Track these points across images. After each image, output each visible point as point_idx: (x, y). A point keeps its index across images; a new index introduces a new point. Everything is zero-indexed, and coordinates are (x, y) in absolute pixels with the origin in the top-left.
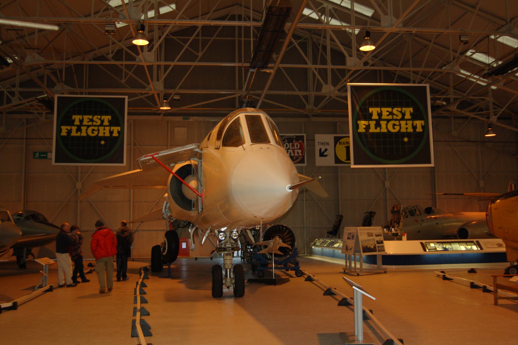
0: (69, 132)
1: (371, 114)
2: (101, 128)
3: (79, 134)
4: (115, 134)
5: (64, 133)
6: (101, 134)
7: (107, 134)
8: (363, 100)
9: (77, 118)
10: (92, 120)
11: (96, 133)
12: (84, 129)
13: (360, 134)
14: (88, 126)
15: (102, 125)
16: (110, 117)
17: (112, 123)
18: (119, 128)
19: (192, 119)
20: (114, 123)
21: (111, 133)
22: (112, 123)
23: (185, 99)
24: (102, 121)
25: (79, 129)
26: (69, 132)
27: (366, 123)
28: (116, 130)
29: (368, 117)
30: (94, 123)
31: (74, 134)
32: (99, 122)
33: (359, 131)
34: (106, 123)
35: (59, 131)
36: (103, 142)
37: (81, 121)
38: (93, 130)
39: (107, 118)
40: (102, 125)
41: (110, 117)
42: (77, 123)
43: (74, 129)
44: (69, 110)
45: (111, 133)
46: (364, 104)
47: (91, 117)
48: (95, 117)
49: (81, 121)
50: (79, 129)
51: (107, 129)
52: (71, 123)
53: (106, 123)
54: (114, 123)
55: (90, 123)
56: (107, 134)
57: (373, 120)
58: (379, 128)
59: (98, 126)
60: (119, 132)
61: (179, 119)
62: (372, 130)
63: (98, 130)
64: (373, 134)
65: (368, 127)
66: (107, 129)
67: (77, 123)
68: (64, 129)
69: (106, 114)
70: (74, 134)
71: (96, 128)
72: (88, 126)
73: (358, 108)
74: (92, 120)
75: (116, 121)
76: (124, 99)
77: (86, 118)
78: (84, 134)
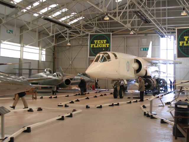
0: (93, 46)
1: (185, 39)
2: (103, 44)
3: (96, 47)
4: (108, 46)
5: (92, 47)
6: (103, 47)
7: (105, 46)
8: (181, 34)
9: (96, 41)
10: (100, 42)
11: (101, 46)
12: (98, 45)
13: (180, 46)
14: (99, 44)
15: (103, 43)
16: (106, 41)
17: (107, 43)
18: (109, 44)
19: (148, 35)
20: (107, 42)
21: (106, 46)
22: (107, 43)
23: (141, 29)
24: (104, 42)
25: (96, 45)
26: (93, 46)
27: (183, 42)
28: (108, 45)
29: (184, 40)
30: (101, 43)
31: (95, 47)
32: (102, 42)
33: (180, 45)
34: (105, 43)
35: (90, 46)
36: (104, 49)
37: (97, 42)
38: (101, 45)
39: (105, 41)
40: (103, 43)
41: (106, 41)
42: (96, 43)
43: (95, 45)
44: (94, 38)
45: (106, 46)
46: (182, 35)
47: (100, 41)
48: (101, 41)
49: (97, 42)
50: (96, 45)
51: (105, 44)
52: (94, 43)
53: (105, 43)
54: (107, 42)
55: (100, 43)
56: (105, 46)
57: (185, 41)
58: (187, 44)
59: (102, 44)
60: (109, 46)
61: (143, 35)
62: (185, 45)
63: (102, 45)
64: (185, 46)
65: (183, 44)
66: (105, 44)
67: (96, 43)
68: (92, 45)
69: (105, 39)
70: (95, 47)
71: (102, 44)
72: (99, 44)
73: (180, 36)
74: (100, 42)
75: (108, 42)
76: (110, 34)
77: (98, 41)
78: (98, 47)
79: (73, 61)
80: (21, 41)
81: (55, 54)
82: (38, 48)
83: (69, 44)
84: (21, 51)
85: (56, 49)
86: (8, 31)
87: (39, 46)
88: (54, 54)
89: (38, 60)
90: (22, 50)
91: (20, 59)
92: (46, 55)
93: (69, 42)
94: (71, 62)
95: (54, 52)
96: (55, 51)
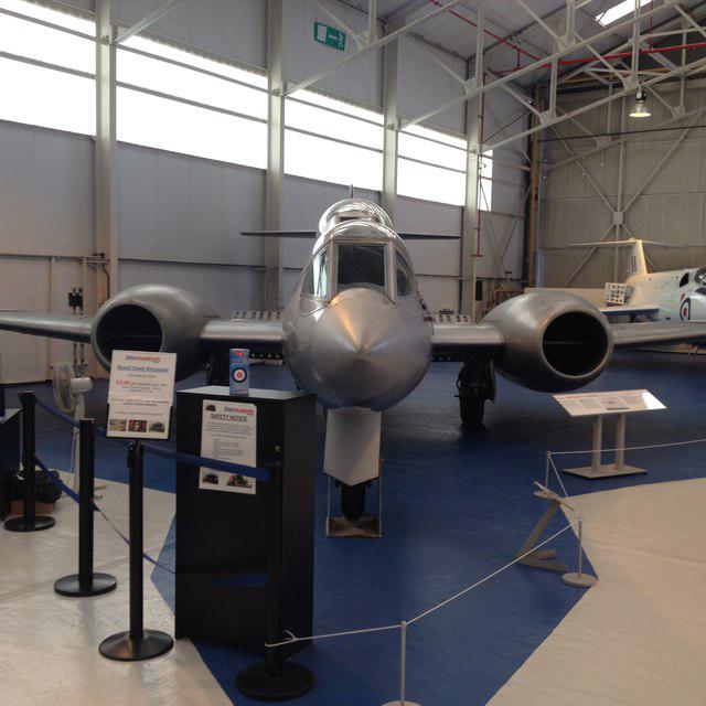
79: (629, 209)
80: (382, 92)
81: (533, 178)
82: (463, 143)
83: (640, 113)
84: (384, 152)
85: (538, 151)
86: (322, 32)
87: (465, 133)
88: (527, 177)
89: (462, 203)
90: (391, 148)
91: (379, 193)
92: (495, 180)
93: (643, 98)
94: (618, 218)
95: (528, 165)
96: (534, 165)
